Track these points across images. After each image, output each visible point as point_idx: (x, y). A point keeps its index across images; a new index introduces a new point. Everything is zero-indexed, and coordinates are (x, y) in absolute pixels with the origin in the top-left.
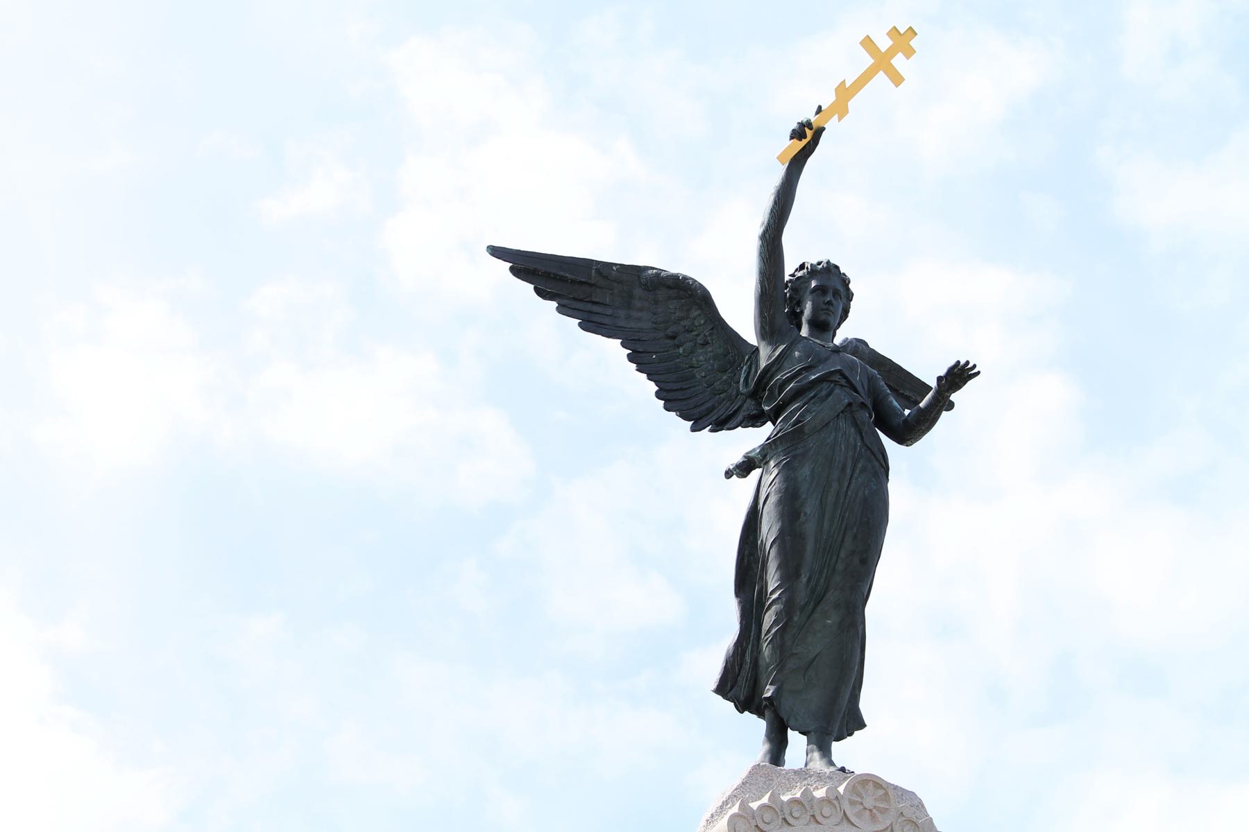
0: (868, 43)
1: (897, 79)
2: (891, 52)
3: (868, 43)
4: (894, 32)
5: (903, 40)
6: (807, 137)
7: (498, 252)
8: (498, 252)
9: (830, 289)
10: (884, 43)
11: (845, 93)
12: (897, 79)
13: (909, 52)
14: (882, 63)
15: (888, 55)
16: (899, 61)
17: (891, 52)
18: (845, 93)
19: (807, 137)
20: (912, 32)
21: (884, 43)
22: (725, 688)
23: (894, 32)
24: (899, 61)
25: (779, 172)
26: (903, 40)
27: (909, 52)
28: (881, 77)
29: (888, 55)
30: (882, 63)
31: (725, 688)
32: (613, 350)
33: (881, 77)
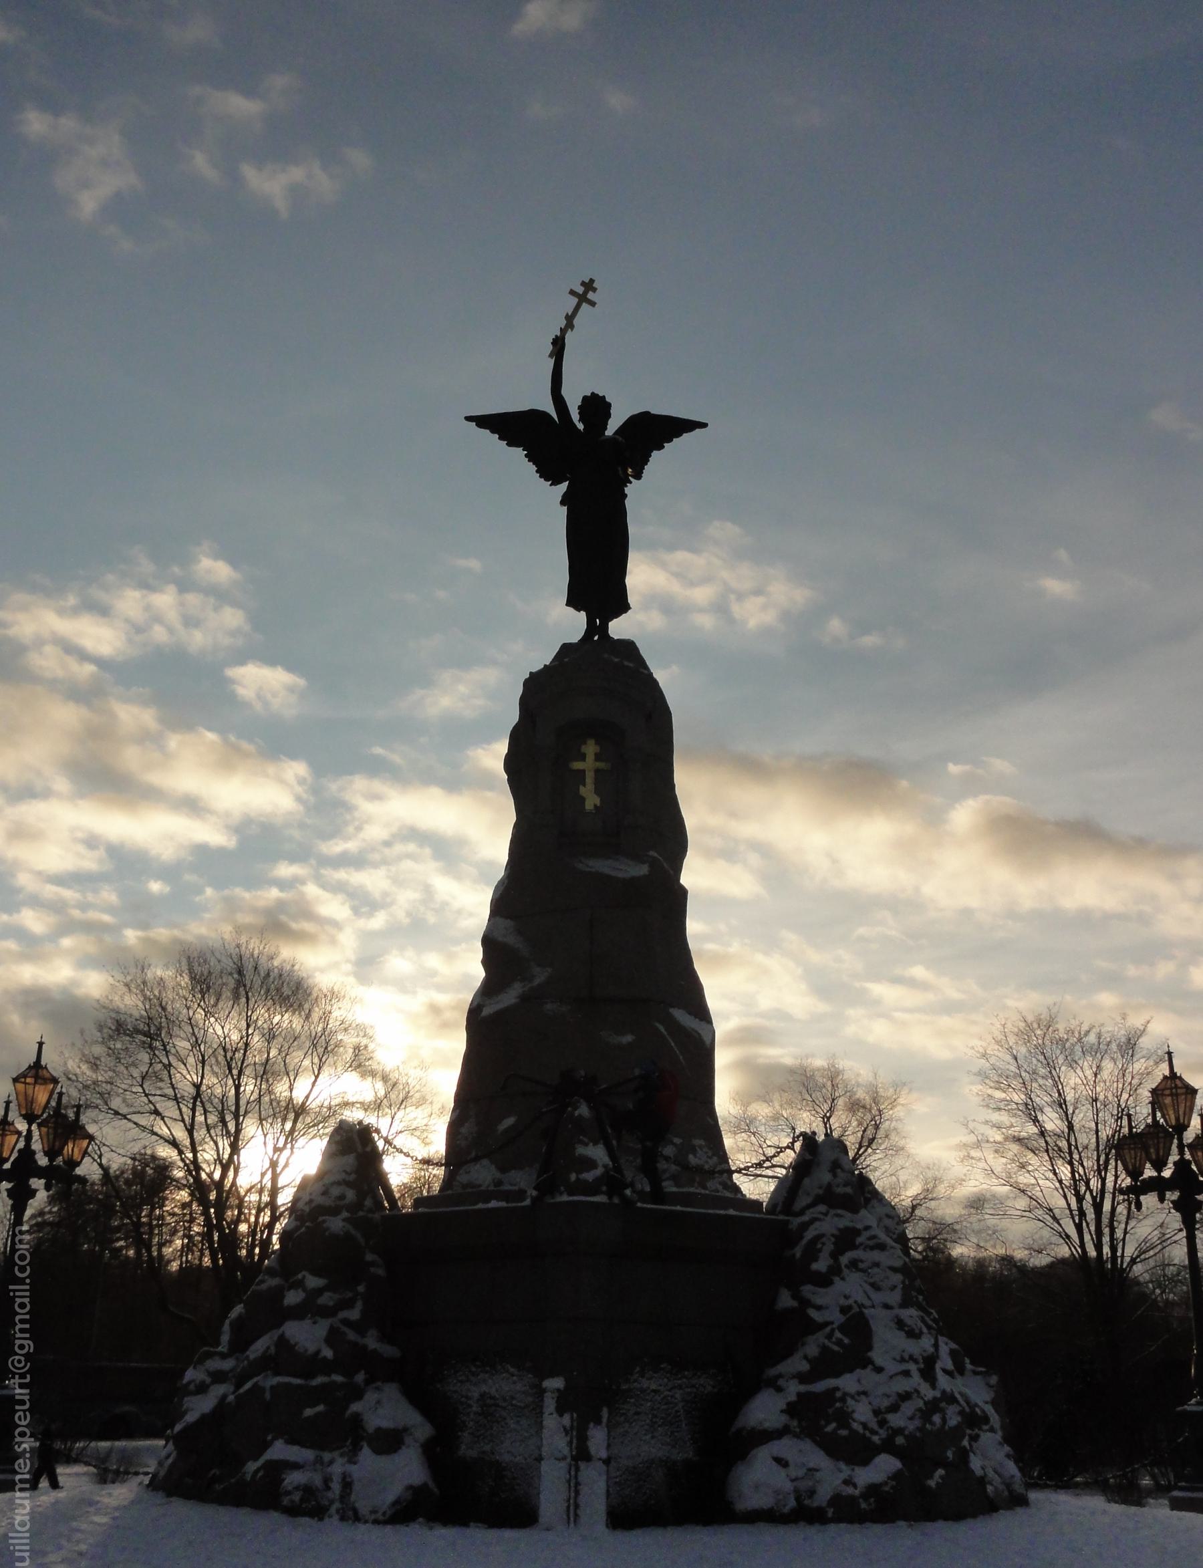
0: (572, 293)
1: (593, 304)
2: (586, 293)
3: (572, 293)
4: (583, 284)
5: (589, 286)
6: (559, 346)
7: (469, 419)
8: (469, 419)
9: (596, 407)
10: (580, 290)
11: (570, 319)
12: (593, 304)
13: (594, 290)
14: (582, 299)
15: (585, 294)
16: (590, 295)
17: (586, 293)
18: (570, 319)
19: (559, 346)
20: (592, 281)
21: (580, 290)
22: (567, 605)
23: (583, 284)
24: (590, 295)
25: (551, 363)
26: (589, 286)
27: (594, 290)
28: (584, 305)
29: (585, 294)
30: (582, 299)
31: (567, 605)
32: (519, 453)
33: (584, 305)
